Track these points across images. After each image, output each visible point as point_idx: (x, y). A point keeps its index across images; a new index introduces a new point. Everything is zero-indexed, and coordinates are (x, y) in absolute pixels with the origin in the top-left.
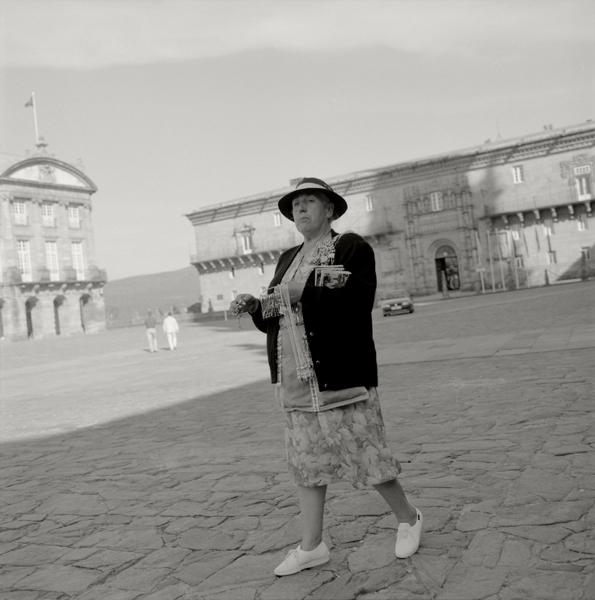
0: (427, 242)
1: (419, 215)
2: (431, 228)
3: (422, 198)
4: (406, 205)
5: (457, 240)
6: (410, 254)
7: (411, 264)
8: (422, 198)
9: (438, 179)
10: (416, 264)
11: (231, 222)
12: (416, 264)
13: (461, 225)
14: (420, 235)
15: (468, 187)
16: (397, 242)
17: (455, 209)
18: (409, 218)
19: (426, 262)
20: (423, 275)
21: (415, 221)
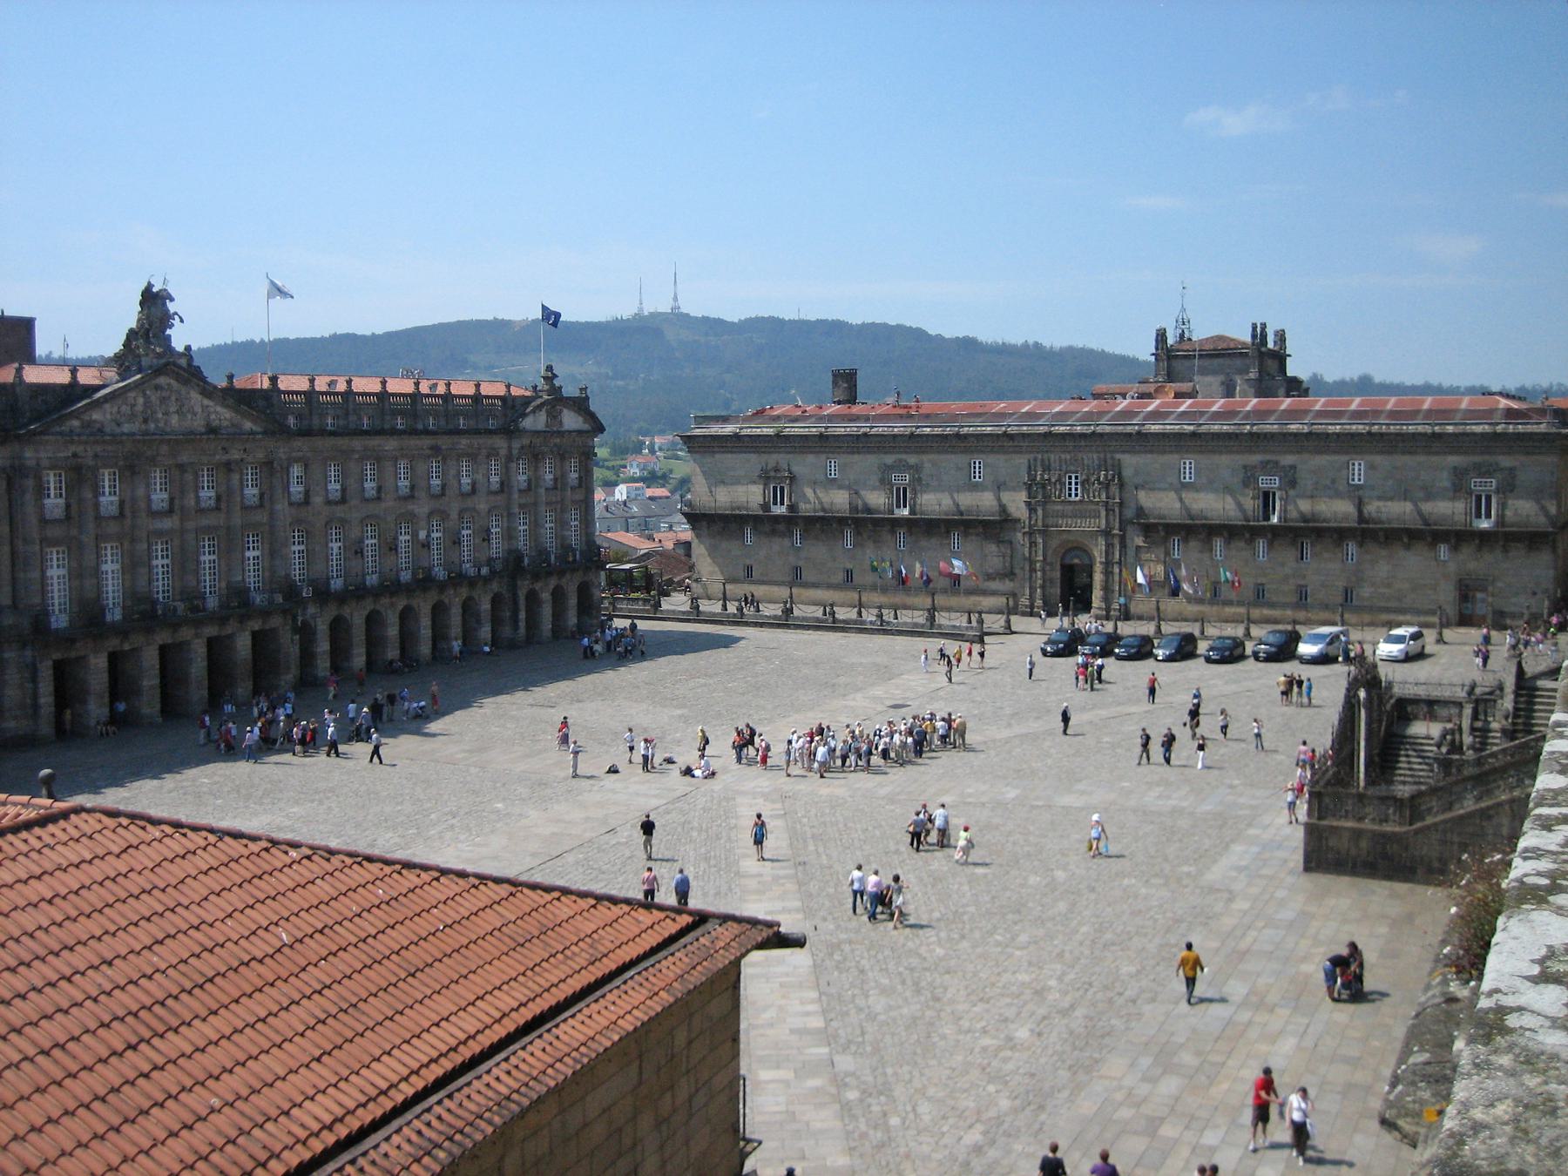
11: (753, 457)
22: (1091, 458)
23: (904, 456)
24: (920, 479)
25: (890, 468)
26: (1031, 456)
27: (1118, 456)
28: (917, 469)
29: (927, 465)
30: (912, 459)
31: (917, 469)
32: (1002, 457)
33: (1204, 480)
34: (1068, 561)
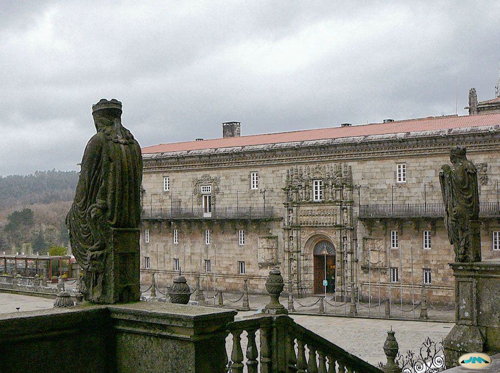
0: (305, 236)
1: (299, 204)
2: (310, 220)
3: (303, 185)
4: (286, 190)
5: (334, 237)
6: (286, 246)
7: (287, 258)
8: (303, 185)
9: (322, 165)
10: (291, 260)
12: (291, 260)
13: (338, 223)
14: (298, 227)
15: (351, 179)
16: (277, 231)
17: (334, 203)
18: (289, 205)
19: (302, 258)
20: (298, 273)
21: (294, 209)
22: (329, 168)
23: (208, 172)
24: (217, 191)
25: (198, 183)
26: (289, 168)
27: (349, 164)
28: (216, 181)
29: (222, 178)
30: (213, 174)
31: (216, 181)
32: (270, 169)
33: (414, 180)
34: (318, 254)
